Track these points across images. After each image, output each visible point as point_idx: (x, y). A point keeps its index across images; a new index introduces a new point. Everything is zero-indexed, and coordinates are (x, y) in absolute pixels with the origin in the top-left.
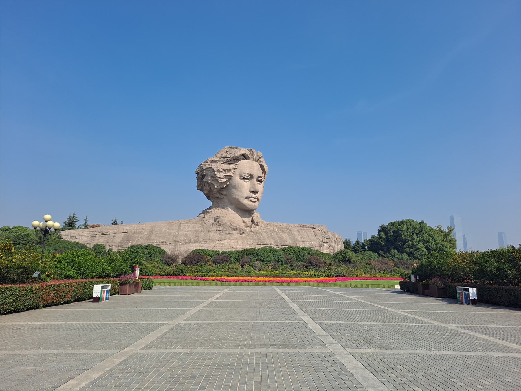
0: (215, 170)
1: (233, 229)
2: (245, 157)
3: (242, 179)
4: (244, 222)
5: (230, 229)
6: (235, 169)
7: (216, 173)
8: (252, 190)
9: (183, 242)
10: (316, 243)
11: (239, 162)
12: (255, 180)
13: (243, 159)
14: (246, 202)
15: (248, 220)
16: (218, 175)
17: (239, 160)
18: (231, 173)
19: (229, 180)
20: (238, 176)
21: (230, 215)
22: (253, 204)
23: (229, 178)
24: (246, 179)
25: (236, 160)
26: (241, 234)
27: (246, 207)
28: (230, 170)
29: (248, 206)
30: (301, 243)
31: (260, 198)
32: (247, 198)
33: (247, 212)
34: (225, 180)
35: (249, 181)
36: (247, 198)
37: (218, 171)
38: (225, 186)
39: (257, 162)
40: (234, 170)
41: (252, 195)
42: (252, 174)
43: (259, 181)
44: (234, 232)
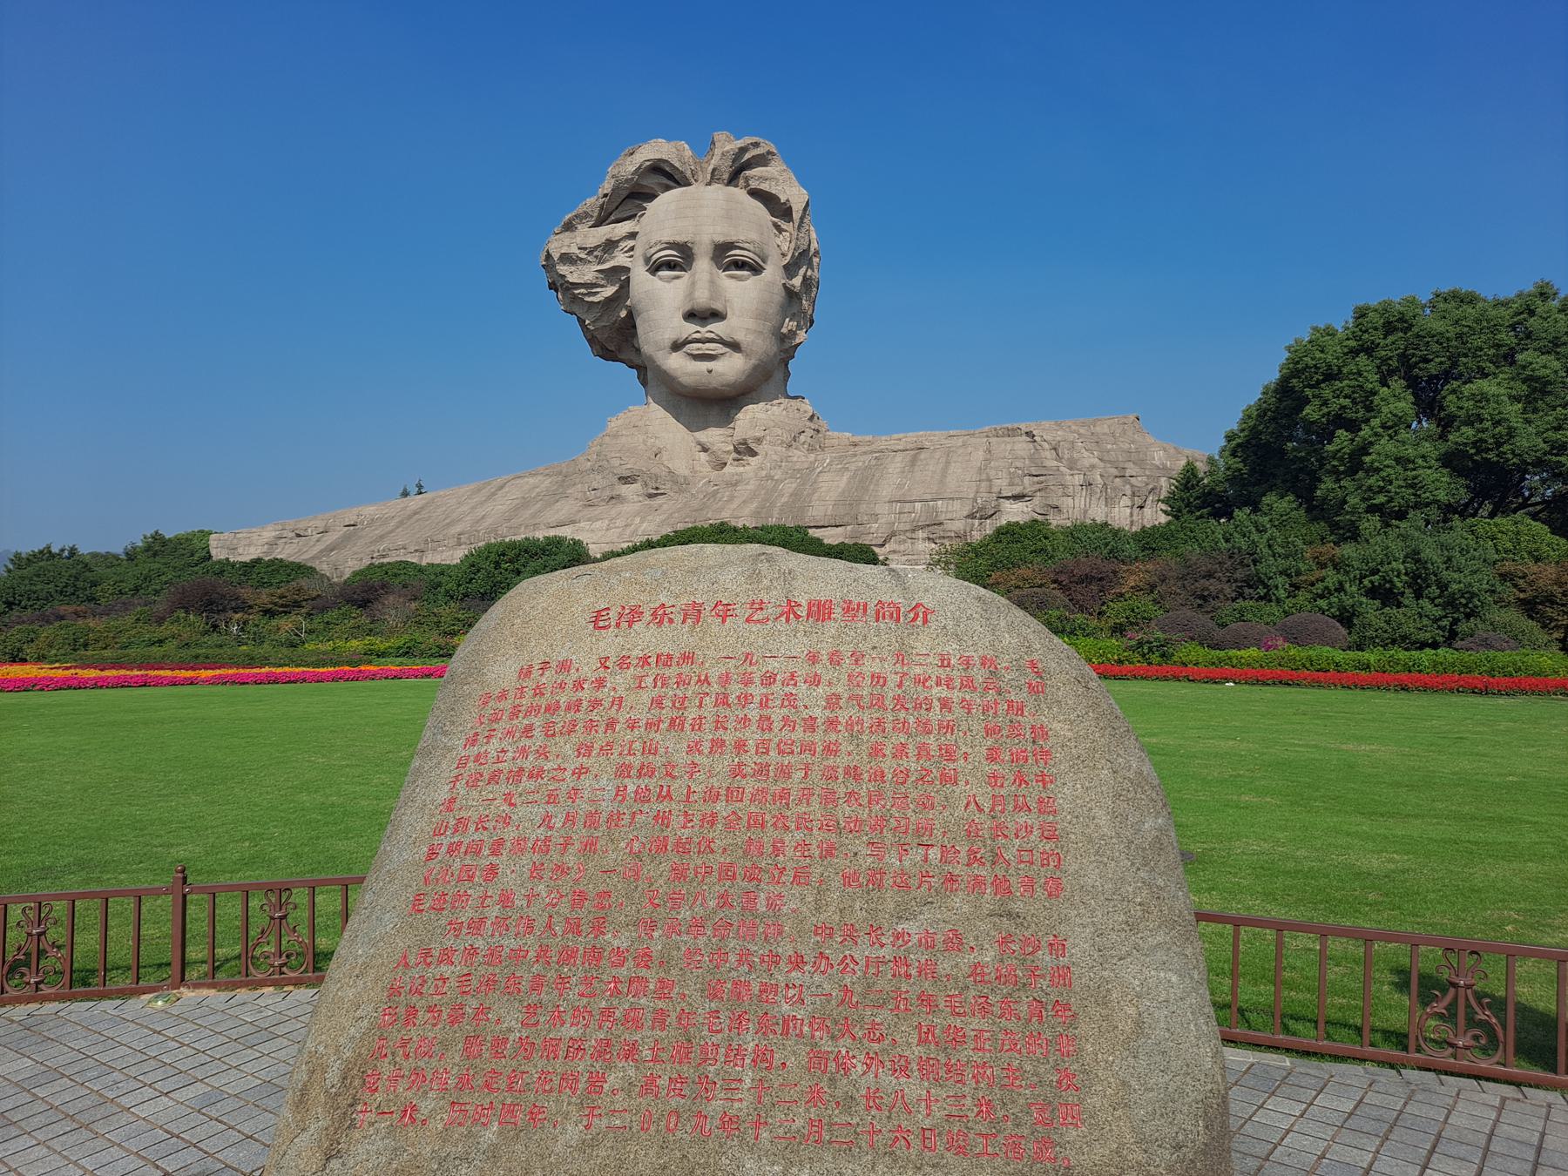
0: (556, 256)
1: (625, 480)
2: (665, 175)
3: (655, 268)
4: (705, 450)
5: (615, 479)
6: (633, 235)
7: (563, 269)
8: (688, 308)
9: (453, 542)
10: (957, 505)
11: (649, 205)
12: (703, 265)
13: (668, 188)
14: (677, 364)
15: (714, 436)
16: (573, 274)
17: (651, 197)
18: (620, 259)
19: (625, 286)
20: (641, 261)
21: (657, 426)
22: (704, 366)
23: (619, 275)
24: (671, 266)
25: (632, 198)
26: (651, 496)
27: (680, 383)
28: (610, 245)
29: (685, 380)
30: (882, 509)
31: (740, 337)
32: (677, 346)
33: (709, 405)
34: (609, 291)
35: (686, 275)
36: (677, 346)
37: (567, 258)
38: (623, 314)
39: (733, 180)
40: (631, 243)
41: (690, 329)
42: (680, 239)
43: (740, 265)
44: (626, 490)
